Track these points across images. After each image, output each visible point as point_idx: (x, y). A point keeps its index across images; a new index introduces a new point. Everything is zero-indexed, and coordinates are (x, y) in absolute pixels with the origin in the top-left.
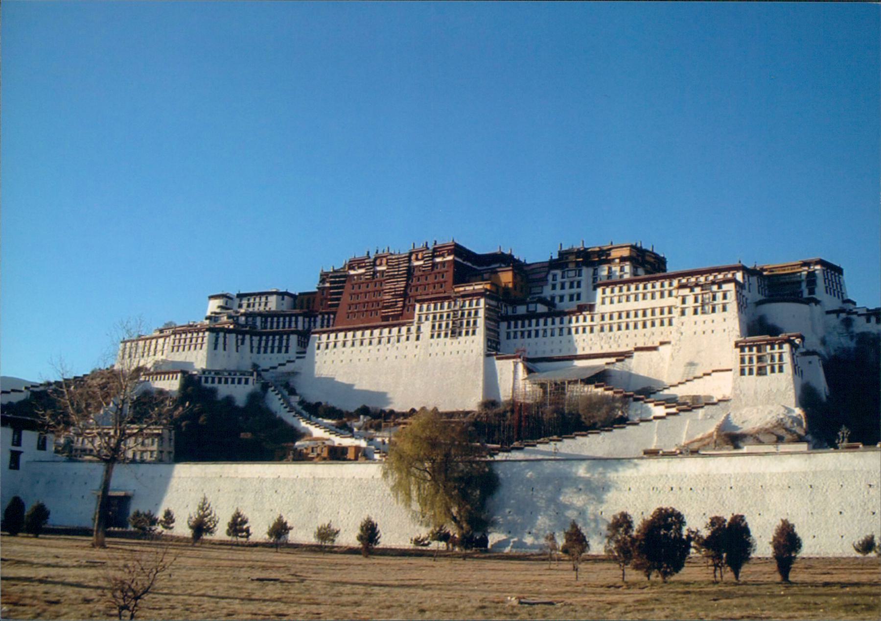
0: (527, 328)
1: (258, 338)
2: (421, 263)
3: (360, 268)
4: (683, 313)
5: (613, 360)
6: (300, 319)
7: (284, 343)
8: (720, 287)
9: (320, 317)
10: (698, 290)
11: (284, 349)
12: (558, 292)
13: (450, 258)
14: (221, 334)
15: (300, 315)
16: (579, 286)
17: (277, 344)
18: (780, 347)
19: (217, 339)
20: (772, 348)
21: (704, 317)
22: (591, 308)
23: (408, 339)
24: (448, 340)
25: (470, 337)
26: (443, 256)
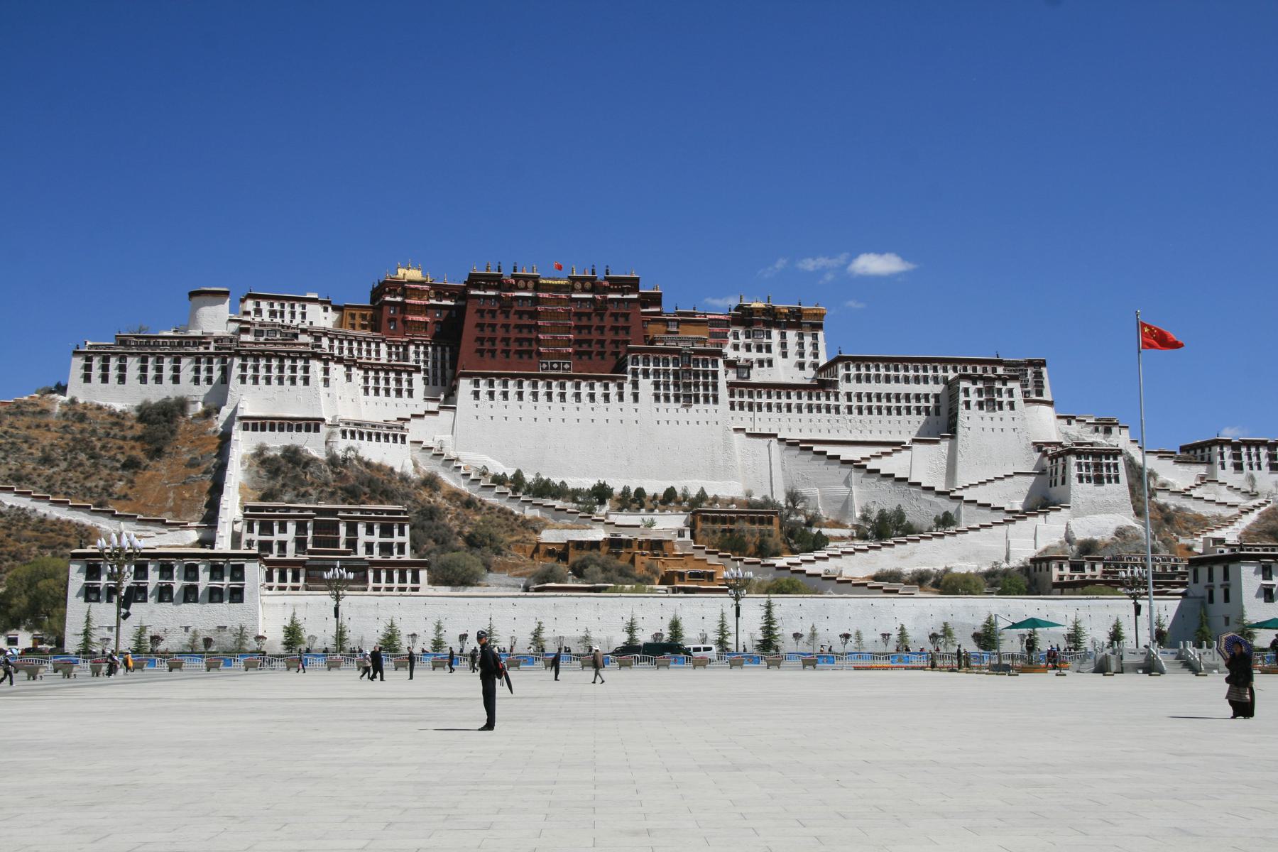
0: (757, 400)
1: (361, 373)
2: (590, 296)
3: (485, 288)
4: (967, 404)
5: (889, 449)
6: (383, 347)
7: (405, 385)
8: (1005, 384)
9: (412, 348)
10: (980, 385)
11: (405, 394)
12: (742, 355)
13: (635, 296)
14: (331, 364)
15: (384, 341)
16: (769, 349)
17: (393, 384)
18: (1115, 458)
19: (326, 371)
20: (1107, 458)
21: (992, 414)
22: (834, 384)
23: (621, 398)
24: (678, 406)
25: (711, 406)
26: (622, 291)
